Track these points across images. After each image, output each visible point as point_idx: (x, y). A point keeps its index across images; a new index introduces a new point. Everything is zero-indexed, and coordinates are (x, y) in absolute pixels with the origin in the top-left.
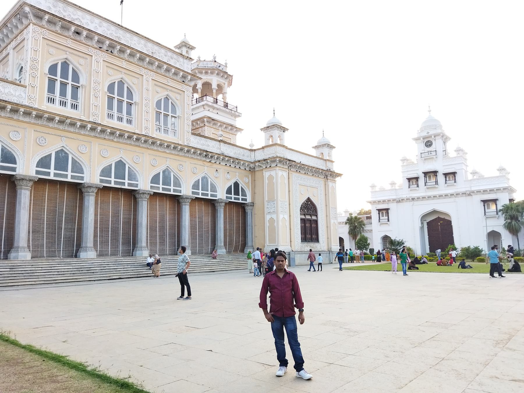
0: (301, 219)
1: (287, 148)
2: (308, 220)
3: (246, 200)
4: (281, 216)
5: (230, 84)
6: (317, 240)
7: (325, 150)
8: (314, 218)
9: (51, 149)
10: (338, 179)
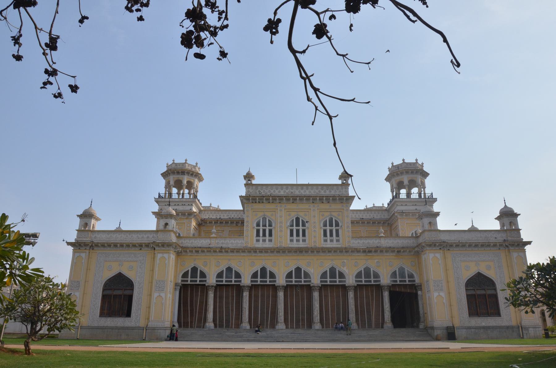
0: (467, 295)
1: (440, 231)
2: (480, 295)
3: (414, 281)
4: (436, 294)
6: (499, 314)
7: (506, 221)
8: (490, 292)
9: (257, 268)
10: (527, 248)
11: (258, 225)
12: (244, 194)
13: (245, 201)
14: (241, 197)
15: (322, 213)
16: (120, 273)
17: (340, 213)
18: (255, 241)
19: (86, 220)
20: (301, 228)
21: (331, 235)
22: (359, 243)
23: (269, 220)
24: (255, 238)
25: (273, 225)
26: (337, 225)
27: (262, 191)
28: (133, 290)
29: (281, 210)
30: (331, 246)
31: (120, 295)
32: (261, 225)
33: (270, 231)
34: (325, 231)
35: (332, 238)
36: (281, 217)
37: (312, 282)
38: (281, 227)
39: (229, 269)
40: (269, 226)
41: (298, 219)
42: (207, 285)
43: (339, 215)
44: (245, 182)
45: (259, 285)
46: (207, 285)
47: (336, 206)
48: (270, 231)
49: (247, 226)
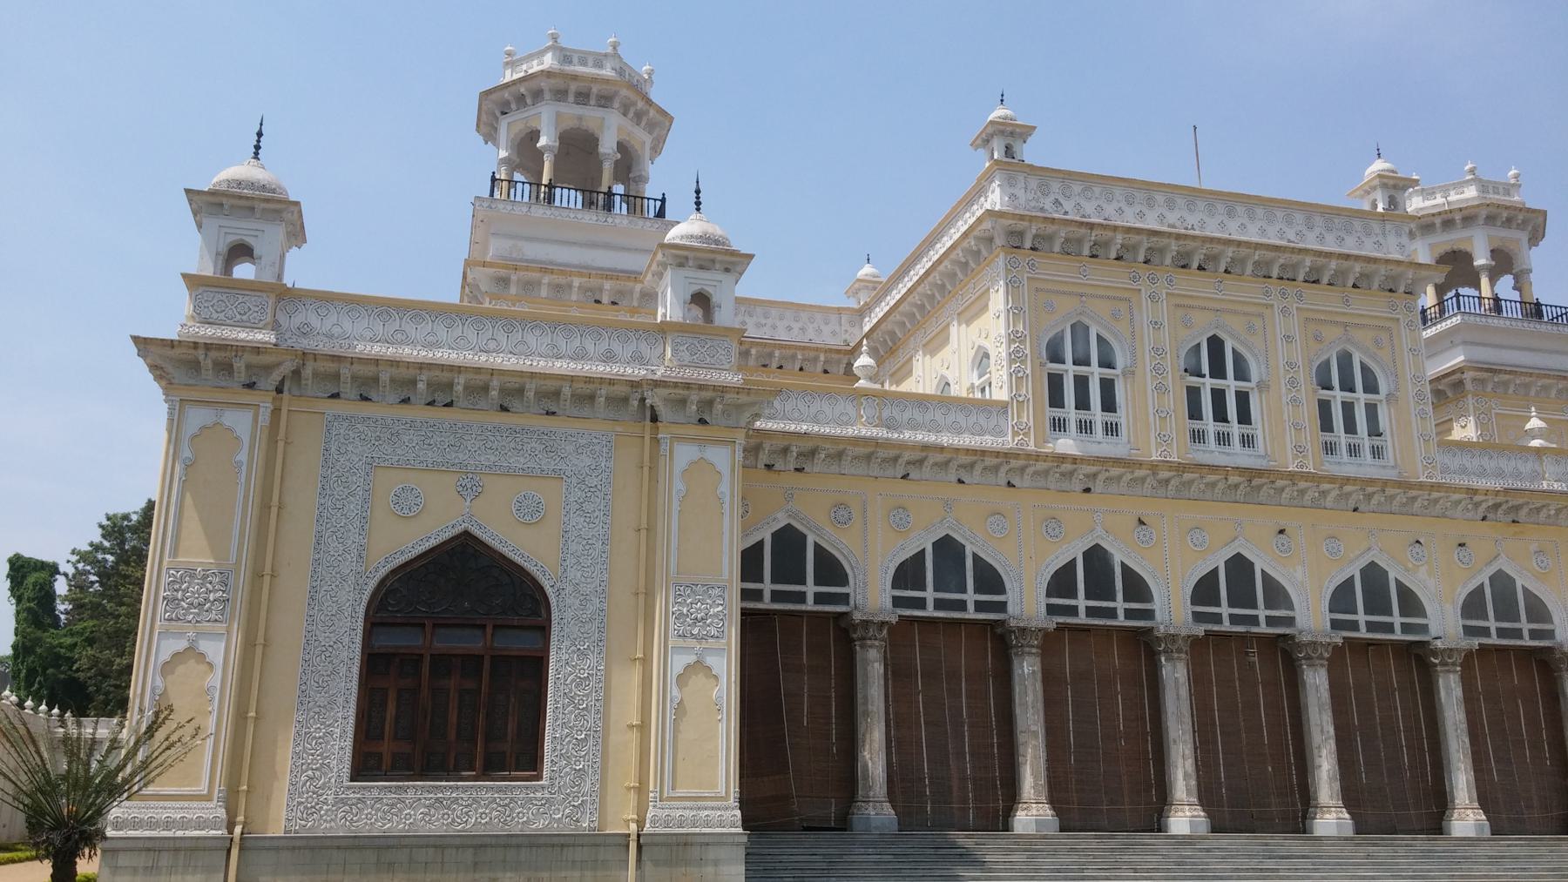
5: (1536, 236)
16: (466, 533)
19: (242, 229)
28: (544, 629)
31: (471, 663)
32: (1069, 357)
37: (1301, 622)
39: (948, 549)
41: (1216, 345)
42: (858, 617)
45: (1085, 629)
46: (858, 617)
47: (1368, 306)
48: (1107, 386)
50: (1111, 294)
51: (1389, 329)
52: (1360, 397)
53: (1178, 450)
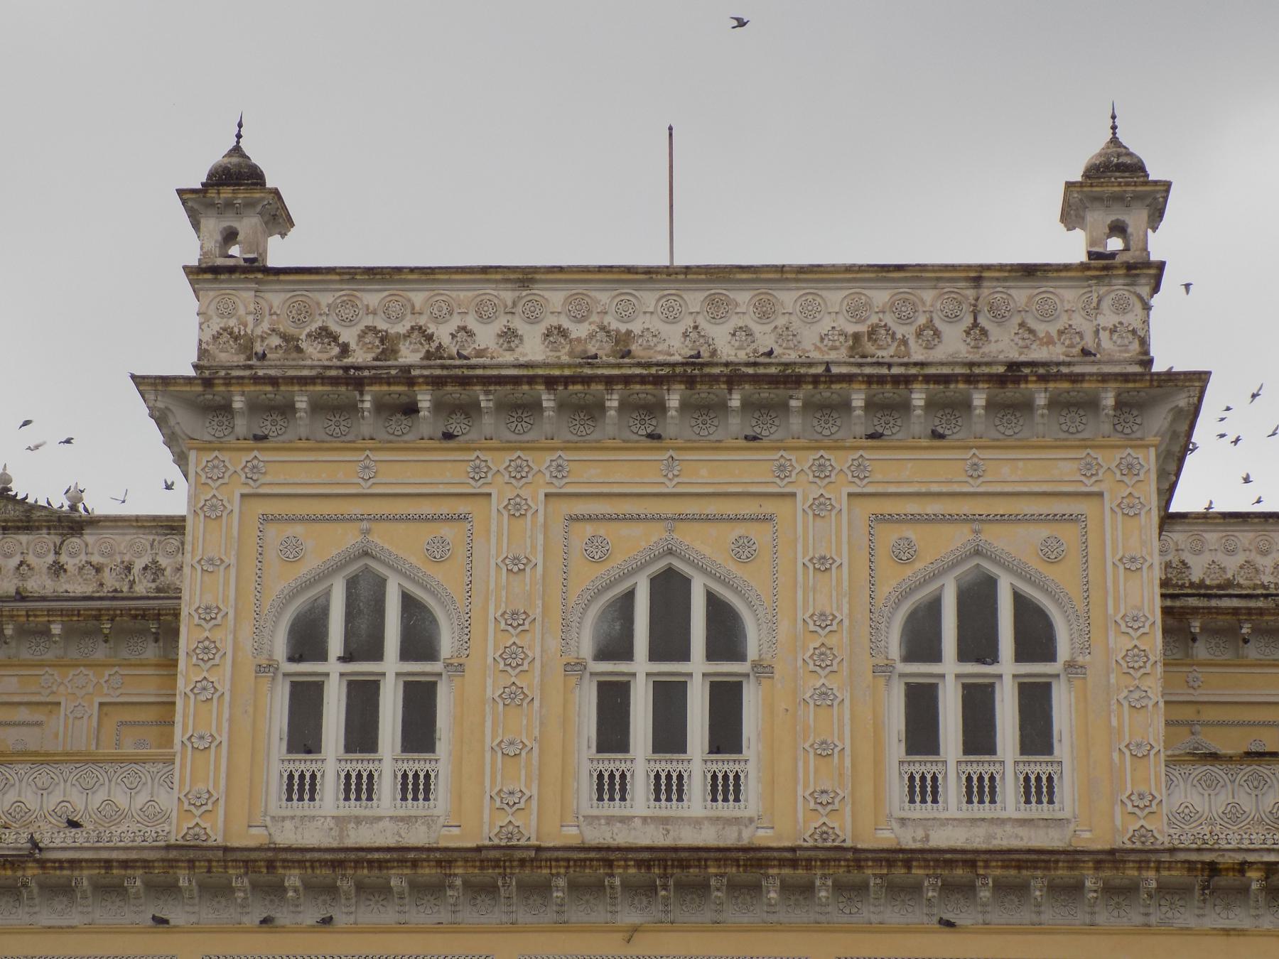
11: (307, 640)
12: (182, 364)
13: (184, 420)
14: (152, 387)
15: (890, 536)
17: (1068, 533)
18: (276, 786)
20: (698, 669)
21: (979, 737)
22: (1234, 815)
23: (410, 604)
24: (277, 761)
25: (447, 644)
26: (1036, 638)
27: (348, 335)
29: (517, 510)
30: (973, 838)
32: (336, 644)
33: (420, 701)
34: (921, 702)
35: (980, 766)
36: (517, 566)
38: (512, 658)
40: (407, 653)
41: (670, 589)
43: (1051, 554)
44: (189, 246)
49: (207, 650)
50: (427, 508)
51: (1072, 519)
52: (1007, 670)
53: (567, 815)
